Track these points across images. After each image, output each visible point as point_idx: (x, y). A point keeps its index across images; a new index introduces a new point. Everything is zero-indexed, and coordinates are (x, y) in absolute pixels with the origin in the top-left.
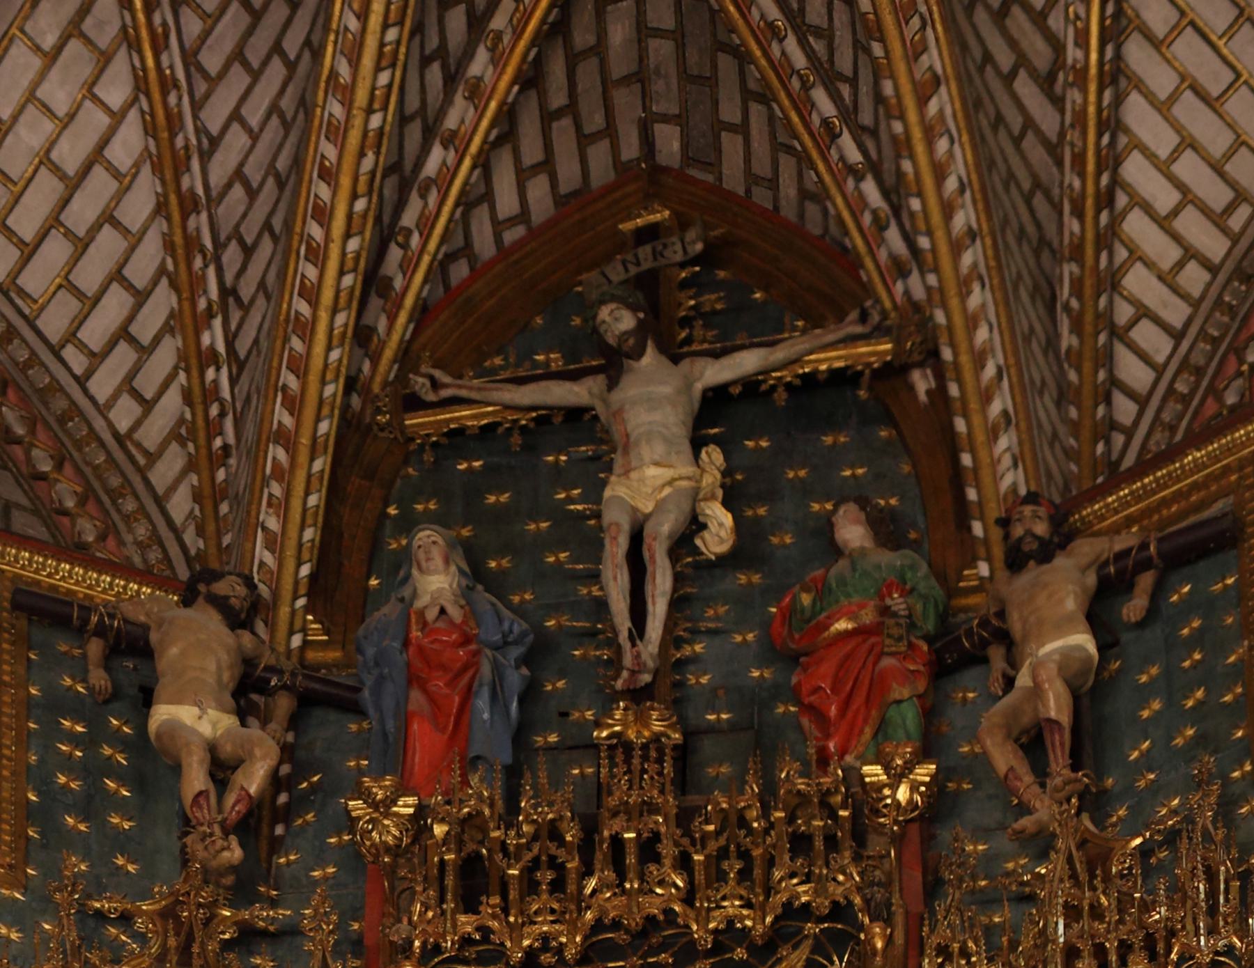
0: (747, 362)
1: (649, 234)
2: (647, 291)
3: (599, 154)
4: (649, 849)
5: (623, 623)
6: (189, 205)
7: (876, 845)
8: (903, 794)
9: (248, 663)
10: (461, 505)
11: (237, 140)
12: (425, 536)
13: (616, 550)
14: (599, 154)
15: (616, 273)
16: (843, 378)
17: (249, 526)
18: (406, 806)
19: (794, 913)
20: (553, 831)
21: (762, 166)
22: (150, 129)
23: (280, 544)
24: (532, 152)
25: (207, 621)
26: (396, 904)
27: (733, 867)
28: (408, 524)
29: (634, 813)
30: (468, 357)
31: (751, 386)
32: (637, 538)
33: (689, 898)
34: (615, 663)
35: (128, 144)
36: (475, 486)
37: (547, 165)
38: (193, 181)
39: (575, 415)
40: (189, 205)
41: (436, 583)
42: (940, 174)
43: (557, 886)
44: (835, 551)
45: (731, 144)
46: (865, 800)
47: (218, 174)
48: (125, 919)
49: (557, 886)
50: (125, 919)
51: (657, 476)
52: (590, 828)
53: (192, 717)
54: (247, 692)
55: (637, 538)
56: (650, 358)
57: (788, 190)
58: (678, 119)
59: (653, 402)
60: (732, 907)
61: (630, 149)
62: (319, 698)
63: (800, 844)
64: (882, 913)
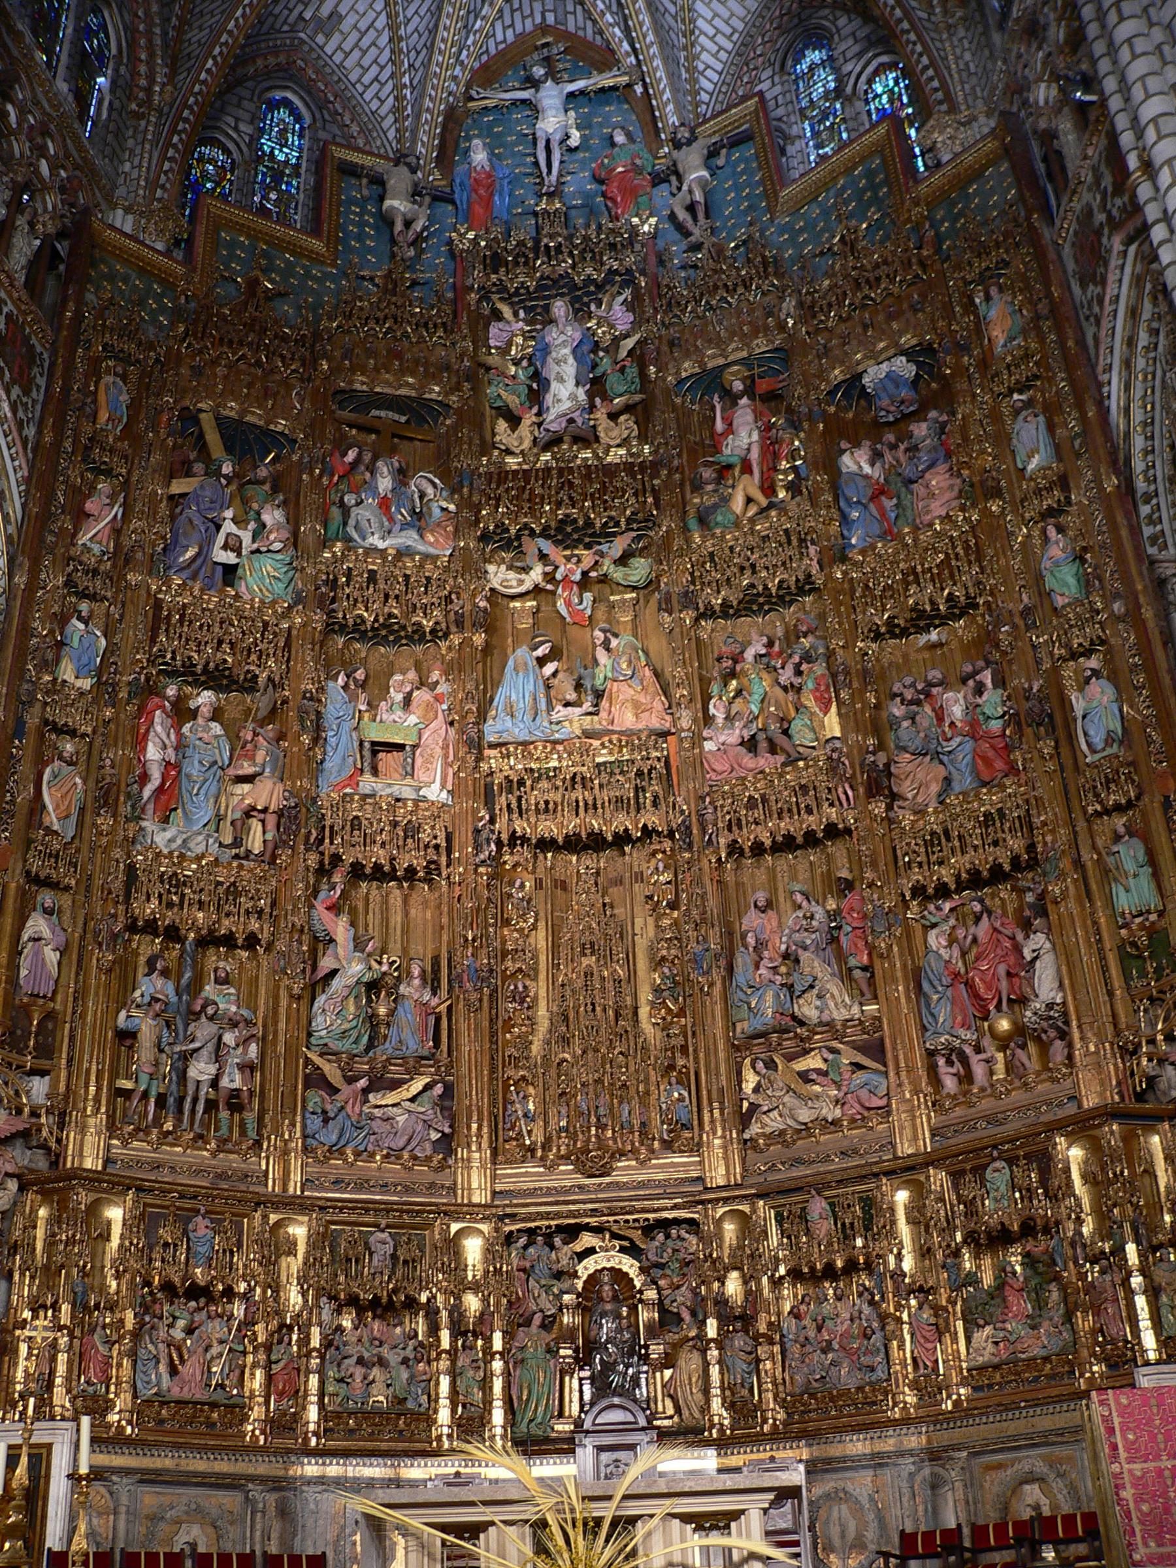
0: (580, 84)
1: (547, 45)
2: (547, 61)
3: (528, 22)
4: (558, 248)
5: (544, 170)
6: (400, 39)
7: (638, 247)
8: (646, 228)
9: (416, 185)
10: (486, 132)
11: (416, 19)
12: (476, 141)
13: (541, 145)
14: (528, 22)
15: (536, 56)
16: (614, 88)
17: (414, 139)
18: (471, 235)
19: (612, 272)
20: (521, 243)
21: (581, 23)
22: (389, 16)
23: (425, 145)
24: (508, 22)
25: (403, 170)
26: (466, 273)
27: (589, 256)
28: (468, 139)
29: (552, 237)
30: (487, 83)
31: (582, 92)
32: (548, 141)
33: (573, 266)
34: (542, 184)
35: (382, 21)
36: (491, 125)
37: (512, 25)
38: (402, 32)
39: (523, 101)
40: (400, 39)
41: (480, 157)
42: (641, 25)
43: (526, 264)
44: (613, 144)
45: (571, 18)
46: (634, 231)
47: (410, 28)
48: (372, 279)
49: (526, 264)
50: (372, 279)
51: (554, 120)
52: (537, 241)
53: (397, 204)
54: (416, 193)
55: (548, 141)
56: (549, 83)
57: (589, 31)
58: (554, 11)
59: (550, 96)
60: (589, 271)
61: (538, 20)
62: (441, 198)
63: (613, 246)
64: (643, 272)
